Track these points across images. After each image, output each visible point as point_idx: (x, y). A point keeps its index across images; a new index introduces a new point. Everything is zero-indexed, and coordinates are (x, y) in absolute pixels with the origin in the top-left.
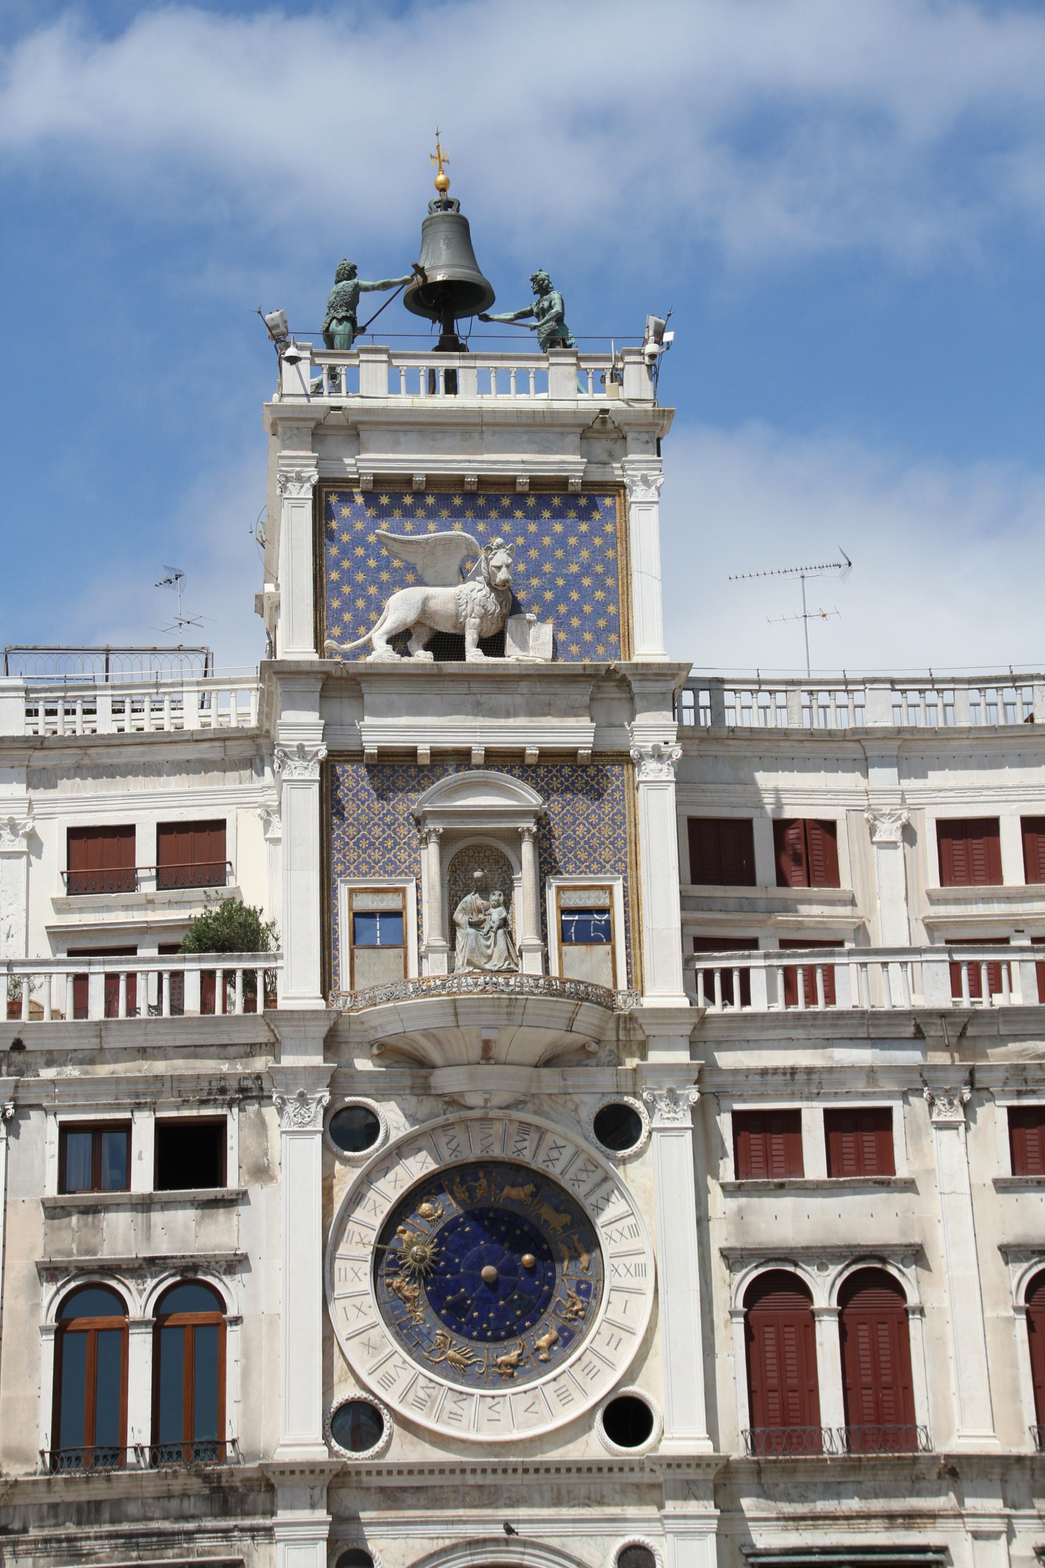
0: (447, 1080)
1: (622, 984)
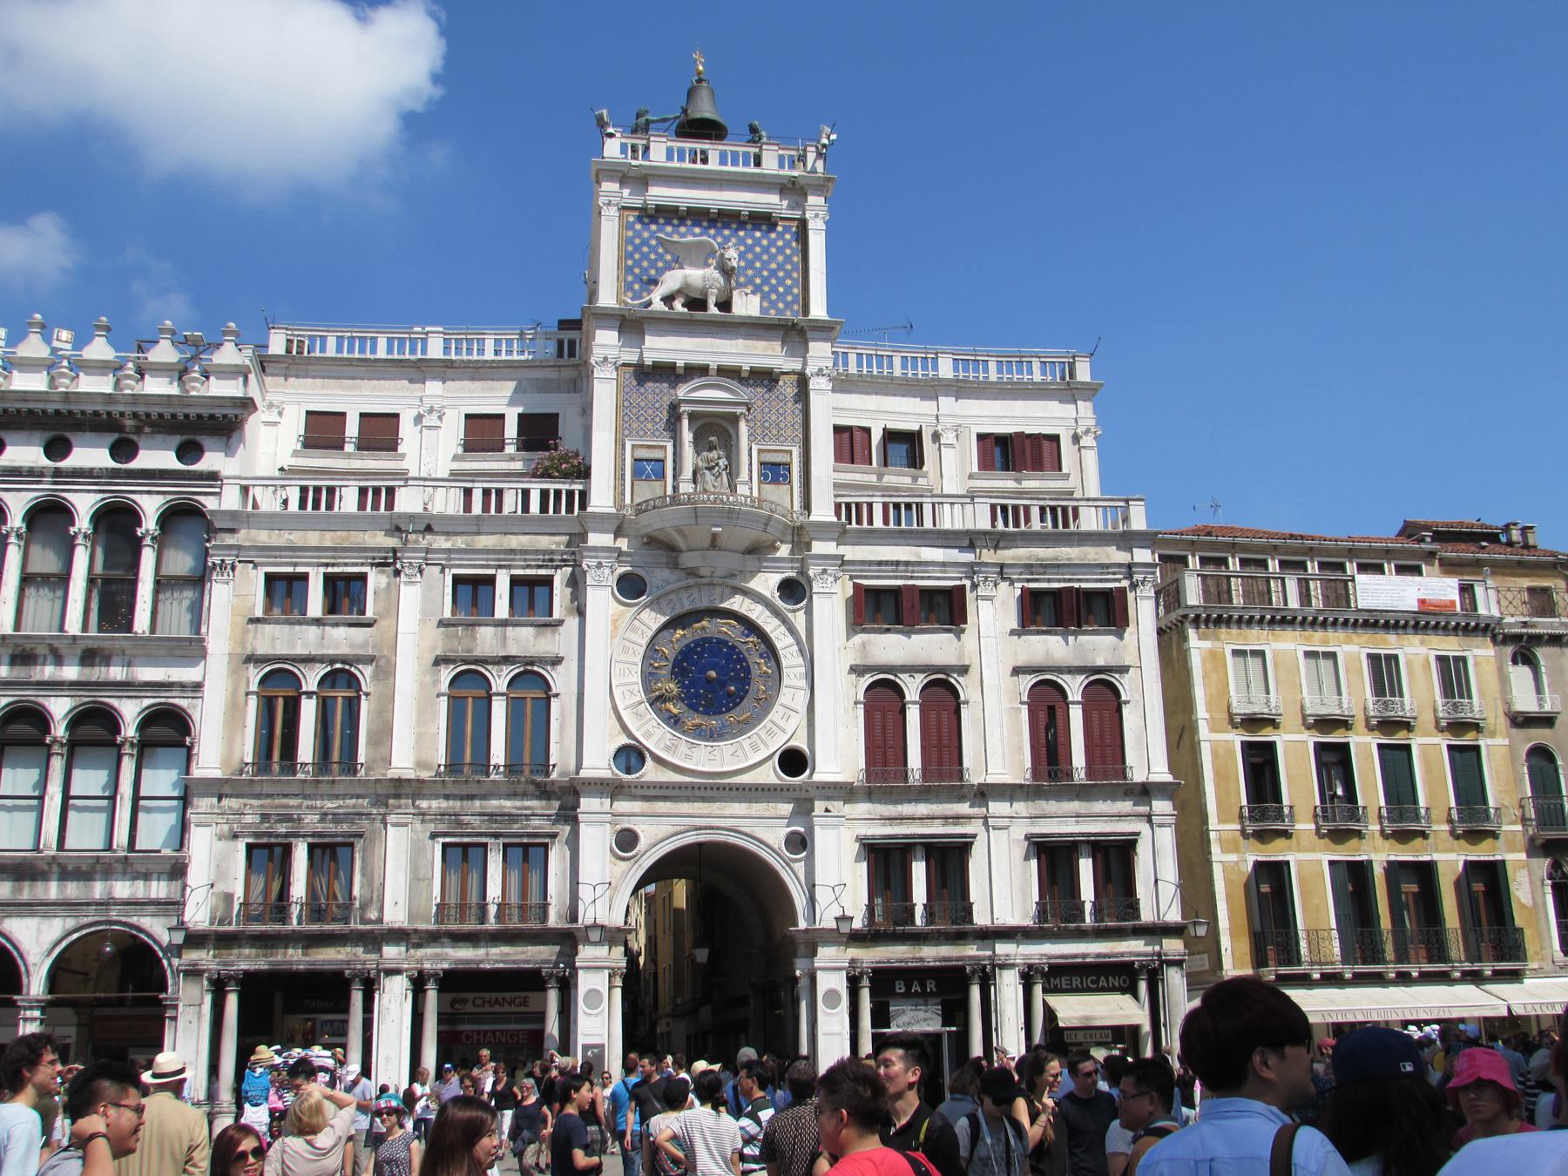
0: (688, 560)
1: (797, 507)
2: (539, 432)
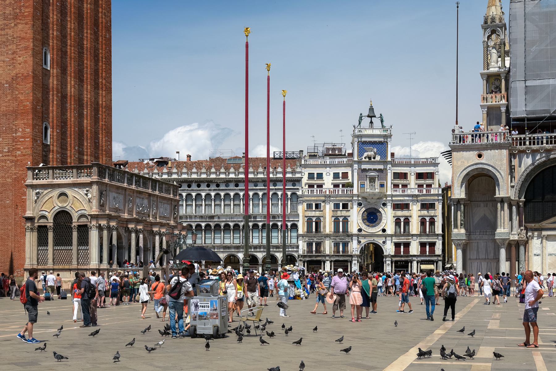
0: (368, 200)
2: (345, 175)
